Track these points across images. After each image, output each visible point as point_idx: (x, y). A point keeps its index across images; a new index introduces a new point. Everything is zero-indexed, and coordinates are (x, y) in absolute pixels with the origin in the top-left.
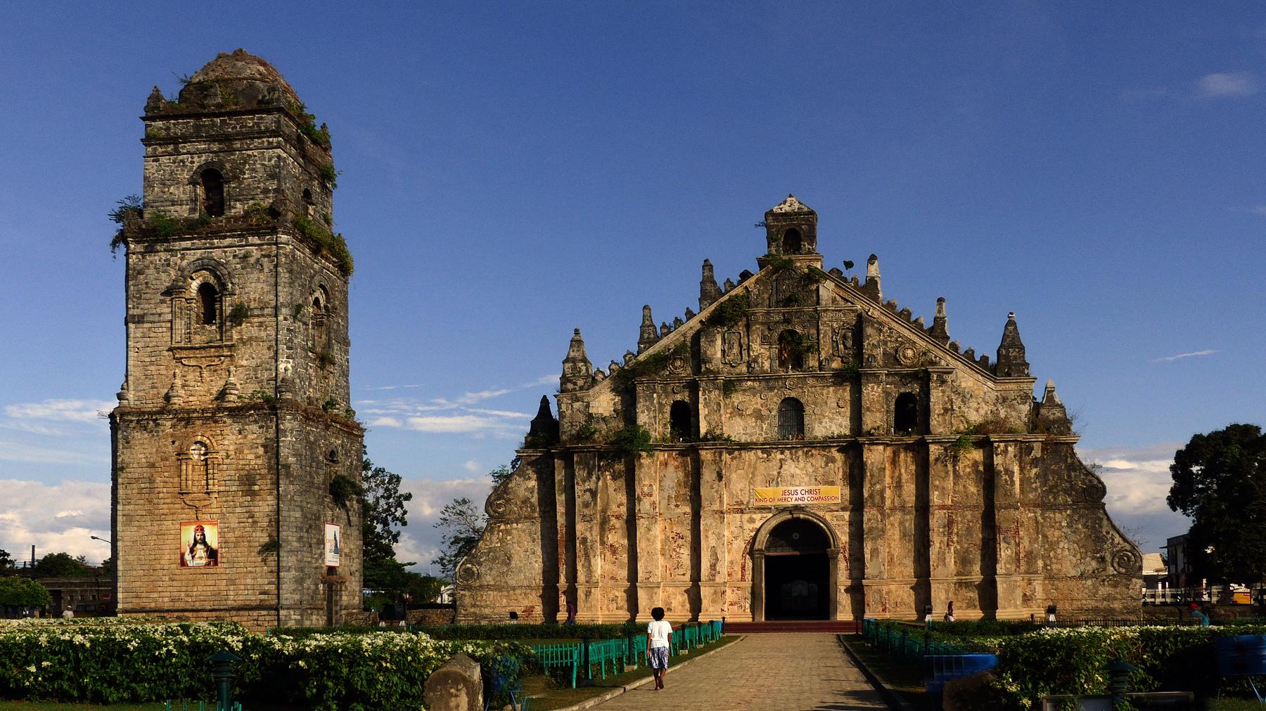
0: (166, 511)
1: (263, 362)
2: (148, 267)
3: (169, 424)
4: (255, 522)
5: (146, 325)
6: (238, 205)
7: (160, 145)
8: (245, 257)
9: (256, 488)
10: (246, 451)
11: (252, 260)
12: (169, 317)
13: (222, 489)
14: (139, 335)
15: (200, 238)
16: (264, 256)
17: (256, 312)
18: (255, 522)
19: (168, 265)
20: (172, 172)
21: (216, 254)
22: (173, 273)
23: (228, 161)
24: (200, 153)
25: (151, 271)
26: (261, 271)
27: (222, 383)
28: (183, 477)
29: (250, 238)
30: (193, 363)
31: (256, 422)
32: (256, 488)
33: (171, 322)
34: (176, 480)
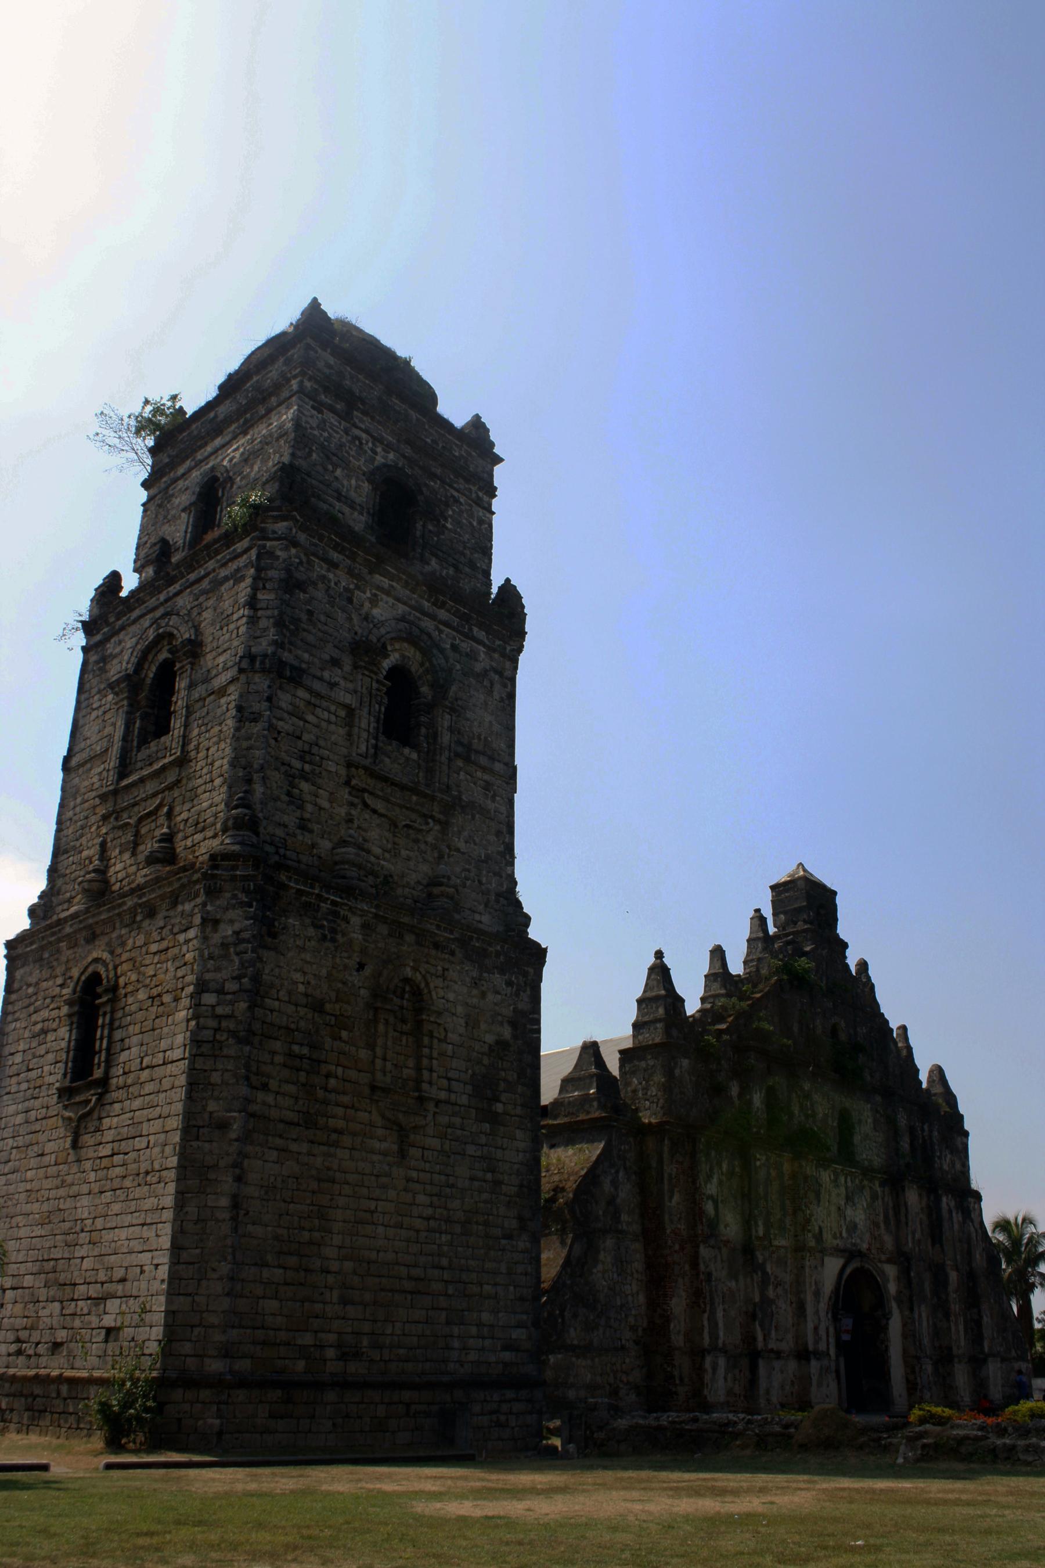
0: (341, 1124)
1: (488, 858)
2: (314, 584)
3: (356, 921)
4: (498, 1183)
5: (301, 693)
6: (434, 562)
7: (326, 390)
8: (467, 655)
9: (499, 1107)
10: (483, 1026)
11: (478, 667)
12: (348, 699)
13: (443, 1095)
14: (283, 705)
15: (406, 585)
16: (496, 671)
17: (483, 760)
18: (498, 1183)
19: (350, 601)
20: (341, 446)
21: (428, 624)
22: (355, 617)
23: (426, 485)
24: (388, 447)
25: (320, 594)
26: (490, 692)
27: (425, 868)
28: (379, 1051)
29: (475, 629)
30: (380, 806)
31: (502, 972)
32: (499, 1107)
33: (350, 711)
34: (364, 1054)
